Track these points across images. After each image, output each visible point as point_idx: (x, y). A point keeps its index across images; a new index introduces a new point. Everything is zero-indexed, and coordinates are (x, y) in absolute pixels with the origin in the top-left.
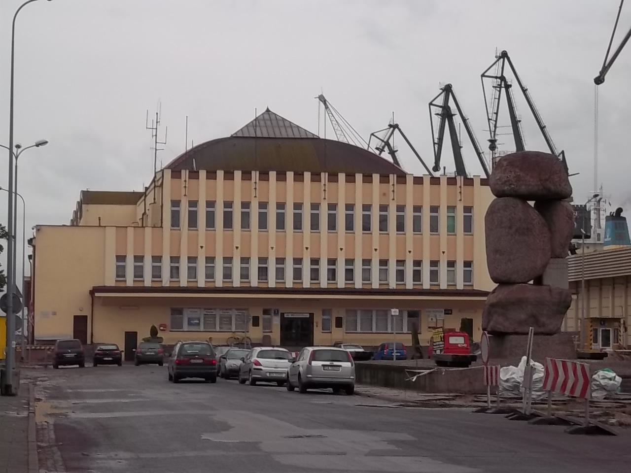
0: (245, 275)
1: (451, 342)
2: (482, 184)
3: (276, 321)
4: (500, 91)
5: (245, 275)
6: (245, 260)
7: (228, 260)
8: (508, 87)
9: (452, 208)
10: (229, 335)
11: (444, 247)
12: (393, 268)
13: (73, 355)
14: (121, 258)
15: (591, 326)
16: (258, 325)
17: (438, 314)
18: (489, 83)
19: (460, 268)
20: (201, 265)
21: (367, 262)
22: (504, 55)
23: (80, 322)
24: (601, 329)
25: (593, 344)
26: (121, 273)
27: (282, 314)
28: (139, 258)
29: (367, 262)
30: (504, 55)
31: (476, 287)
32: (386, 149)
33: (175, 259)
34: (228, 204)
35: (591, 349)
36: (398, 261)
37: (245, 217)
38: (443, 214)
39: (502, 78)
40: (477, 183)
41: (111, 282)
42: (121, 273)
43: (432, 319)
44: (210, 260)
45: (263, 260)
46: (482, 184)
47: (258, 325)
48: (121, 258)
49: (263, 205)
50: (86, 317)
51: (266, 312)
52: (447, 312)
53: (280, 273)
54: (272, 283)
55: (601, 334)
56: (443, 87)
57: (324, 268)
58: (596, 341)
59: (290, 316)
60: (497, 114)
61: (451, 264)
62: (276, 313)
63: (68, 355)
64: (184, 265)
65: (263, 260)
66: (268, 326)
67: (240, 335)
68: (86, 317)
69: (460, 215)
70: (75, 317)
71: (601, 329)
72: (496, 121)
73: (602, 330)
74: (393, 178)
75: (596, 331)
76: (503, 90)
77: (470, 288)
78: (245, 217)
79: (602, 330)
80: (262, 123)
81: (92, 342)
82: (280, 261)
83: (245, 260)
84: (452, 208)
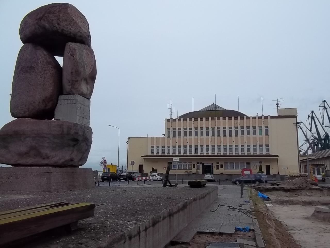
0: (191, 151)
1: (245, 173)
2: (271, 118)
3: (201, 166)
4: (324, 110)
5: (191, 151)
6: (191, 146)
7: (185, 146)
8: (326, 109)
9: (260, 127)
10: (185, 170)
11: (258, 140)
12: (240, 148)
13: (106, 177)
14: (153, 147)
15: (312, 167)
16: (195, 167)
17: (257, 163)
18: (321, 108)
19: (264, 147)
20: (177, 148)
21: (231, 146)
22: (325, 101)
23: (141, 167)
24: (316, 168)
25: (313, 174)
26: (152, 151)
27: (203, 164)
28: (158, 147)
29: (231, 146)
30: (325, 101)
31: (270, 154)
32: (300, 128)
33: (169, 147)
34: (185, 129)
35: (312, 176)
36: (241, 145)
37: (191, 133)
38: (257, 129)
39: (325, 107)
40: (269, 118)
41: (149, 154)
42: (152, 151)
43: (255, 165)
44: (180, 147)
45: (196, 146)
46: (271, 118)
47: (195, 167)
48: (153, 147)
49: (196, 129)
50: (142, 165)
51: (198, 163)
52: (260, 163)
53: (202, 150)
54: (199, 153)
55: (316, 170)
56: (311, 111)
57: (216, 148)
58: (314, 173)
59: (206, 164)
60: (324, 116)
61: (261, 146)
62: (201, 163)
63: (105, 177)
64: (171, 148)
65: (196, 146)
66: (198, 168)
67: (189, 171)
68: (142, 165)
69: (263, 128)
70: (139, 165)
71: (316, 168)
72: (324, 117)
73: (317, 169)
74: (239, 118)
75: (314, 169)
76: (325, 110)
77: (268, 154)
78: (191, 133)
79: (317, 169)
80: (210, 107)
81: (144, 173)
82: (202, 146)
83: (191, 146)
84: (260, 127)
